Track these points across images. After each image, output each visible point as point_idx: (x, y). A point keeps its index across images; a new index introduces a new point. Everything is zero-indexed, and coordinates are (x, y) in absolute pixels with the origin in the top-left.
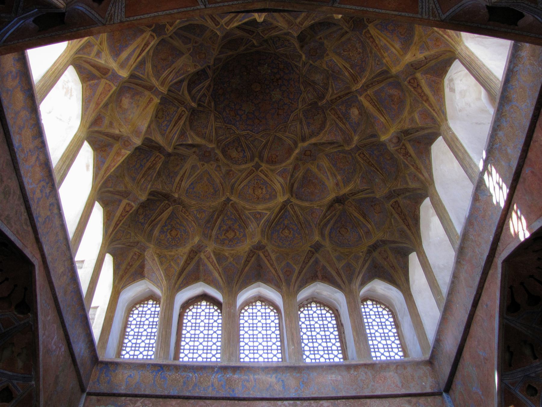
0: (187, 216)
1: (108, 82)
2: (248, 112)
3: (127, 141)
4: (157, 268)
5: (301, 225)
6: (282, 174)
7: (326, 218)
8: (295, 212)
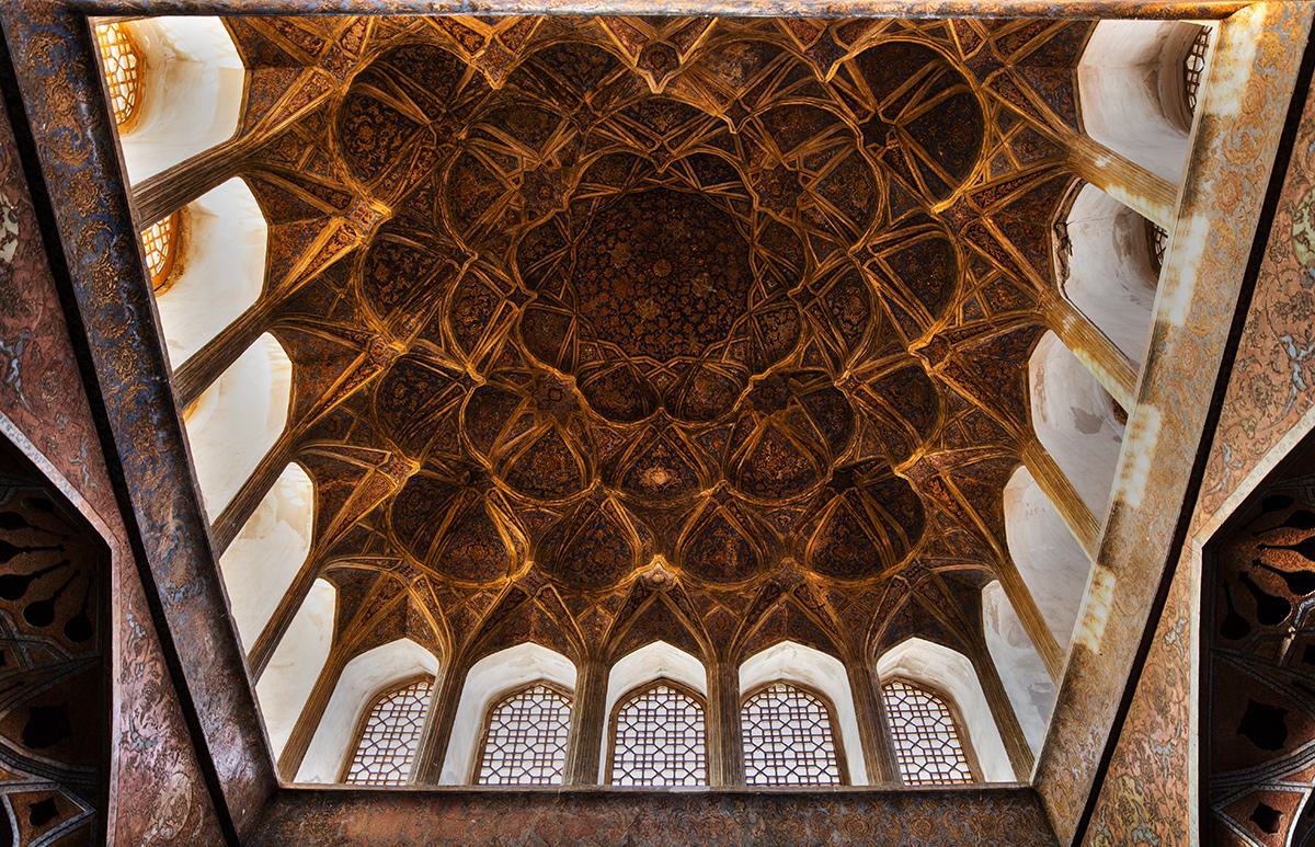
0: (416, 167)
1: (820, 34)
2: (610, 256)
3: (665, 62)
4: (291, 109)
5: (421, 419)
6: (509, 350)
7: (444, 463)
8: (447, 399)
